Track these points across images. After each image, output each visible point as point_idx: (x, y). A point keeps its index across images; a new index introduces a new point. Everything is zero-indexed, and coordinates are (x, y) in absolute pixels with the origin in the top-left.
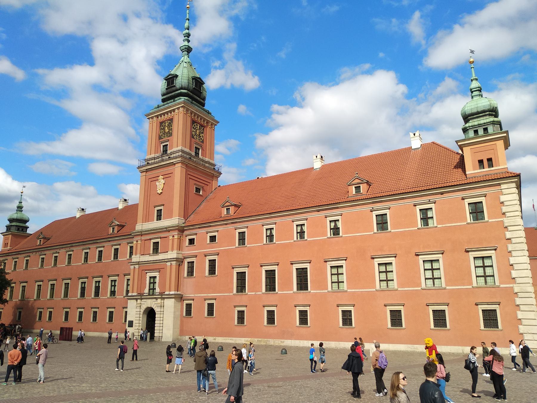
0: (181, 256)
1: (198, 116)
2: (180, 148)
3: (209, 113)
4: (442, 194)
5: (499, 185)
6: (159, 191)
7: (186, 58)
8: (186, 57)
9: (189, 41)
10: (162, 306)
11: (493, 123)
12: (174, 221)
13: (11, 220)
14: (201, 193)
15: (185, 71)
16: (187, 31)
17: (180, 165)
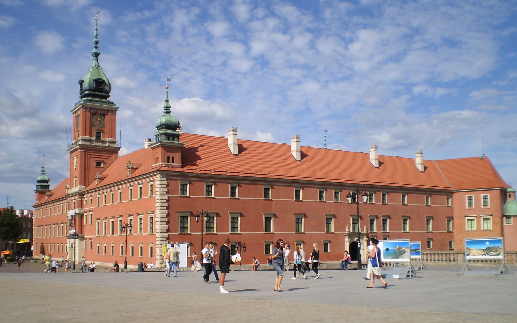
0: (82, 211)
1: (98, 109)
2: (80, 138)
3: (109, 103)
4: (144, 178)
5: (156, 175)
6: (75, 167)
7: (94, 63)
8: (94, 61)
9: (97, 48)
10: (75, 243)
11: (160, 134)
12: (76, 189)
13: (39, 181)
14: (102, 166)
15: (89, 76)
16: (95, 40)
17: (79, 150)
